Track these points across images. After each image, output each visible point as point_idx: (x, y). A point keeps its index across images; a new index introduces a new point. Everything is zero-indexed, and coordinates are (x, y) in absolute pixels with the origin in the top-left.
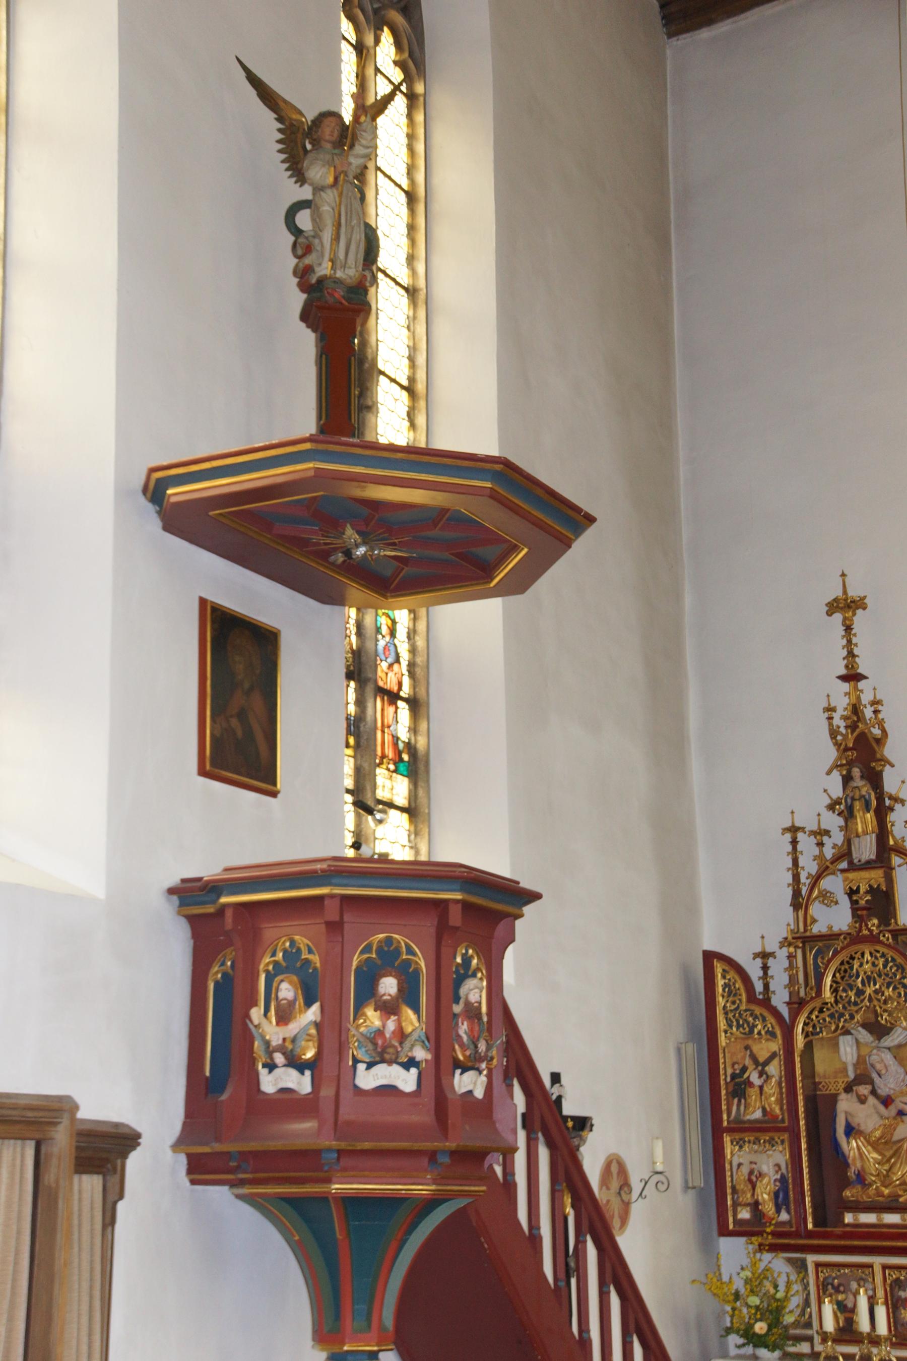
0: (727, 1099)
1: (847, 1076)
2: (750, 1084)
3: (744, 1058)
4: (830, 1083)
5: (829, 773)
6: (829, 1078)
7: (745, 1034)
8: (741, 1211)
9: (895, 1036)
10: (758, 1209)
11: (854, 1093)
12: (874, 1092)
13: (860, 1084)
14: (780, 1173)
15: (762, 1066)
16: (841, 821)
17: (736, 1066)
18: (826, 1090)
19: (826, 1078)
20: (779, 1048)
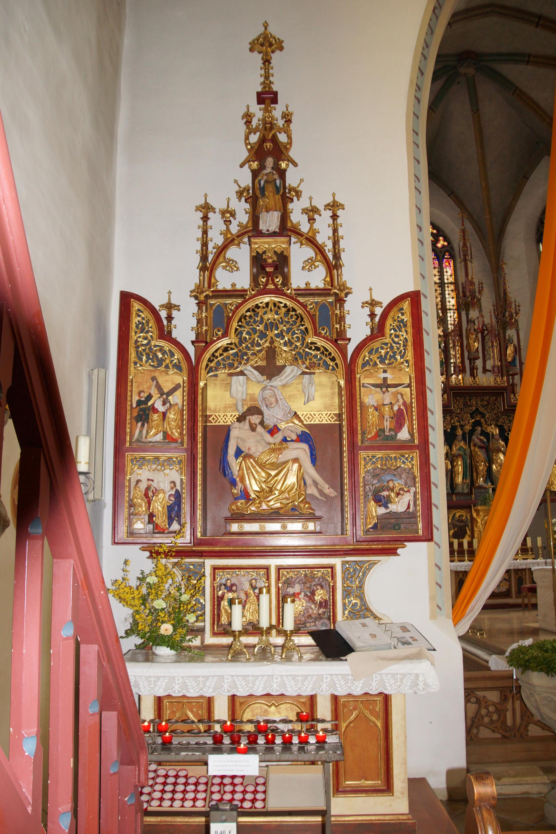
0: (131, 423)
1: (237, 410)
2: (155, 411)
3: (150, 387)
4: (220, 416)
5: (242, 166)
6: (219, 412)
7: (153, 366)
8: (136, 522)
9: (283, 377)
10: (153, 520)
11: (247, 421)
12: (262, 423)
13: (252, 415)
14: (174, 490)
15: (165, 395)
16: (247, 206)
17: (142, 394)
18: (215, 422)
19: (216, 412)
20: (183, 380)
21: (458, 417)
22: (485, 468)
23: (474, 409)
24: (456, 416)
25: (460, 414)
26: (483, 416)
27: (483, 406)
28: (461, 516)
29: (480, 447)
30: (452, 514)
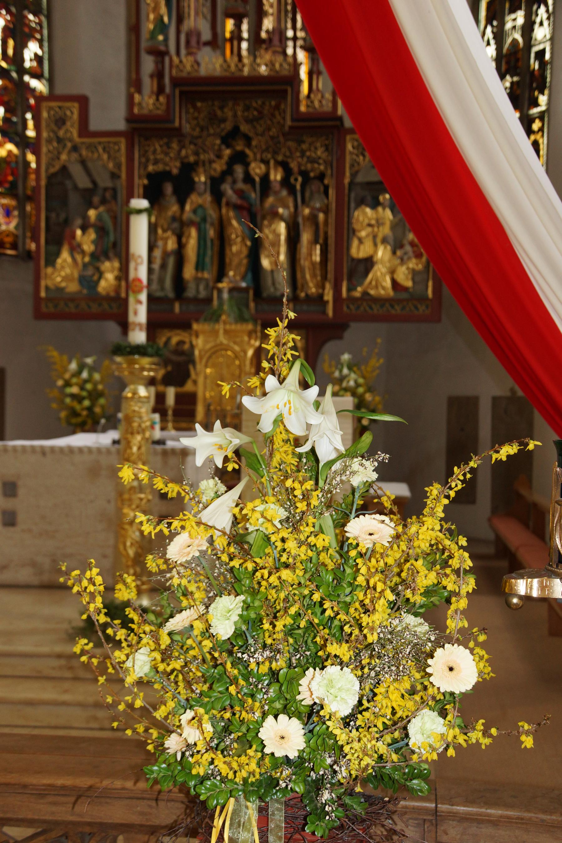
21: (195, 145)
22: (245, 252)
23: (228, 126)
24: (191, 143)
25: (200, 137)
26: (248, 140)
27: (248, 121)
28: (181, 343)
29: (237, 208)
30: (164, 339)
